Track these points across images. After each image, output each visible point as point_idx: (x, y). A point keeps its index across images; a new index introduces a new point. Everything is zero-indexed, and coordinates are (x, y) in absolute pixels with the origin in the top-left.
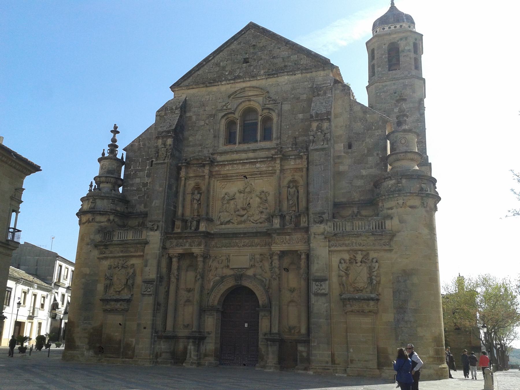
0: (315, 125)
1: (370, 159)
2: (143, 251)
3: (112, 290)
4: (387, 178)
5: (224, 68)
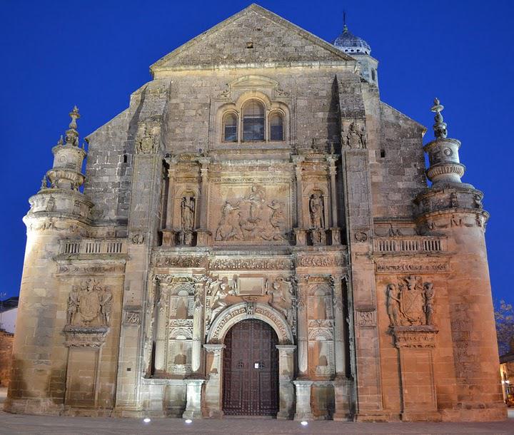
0: (346, 124)
2: (123, 269)
3: (78, 320)
4: (439, 191)
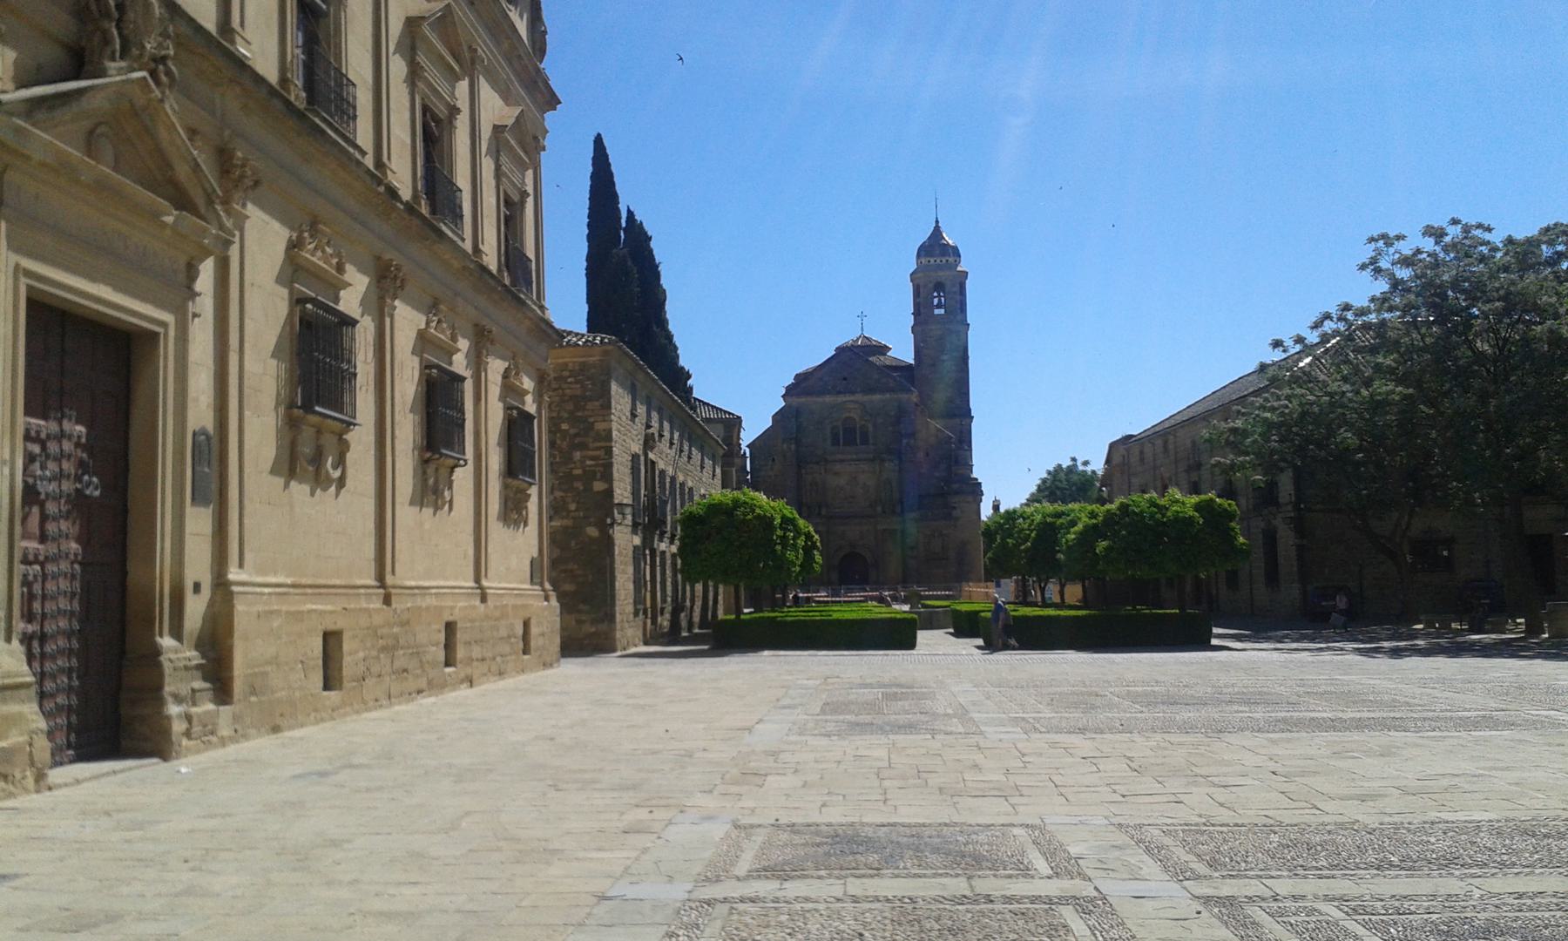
0: (905, 441)
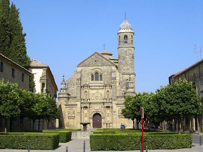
1: (124, 87)
5: (90, 62)
